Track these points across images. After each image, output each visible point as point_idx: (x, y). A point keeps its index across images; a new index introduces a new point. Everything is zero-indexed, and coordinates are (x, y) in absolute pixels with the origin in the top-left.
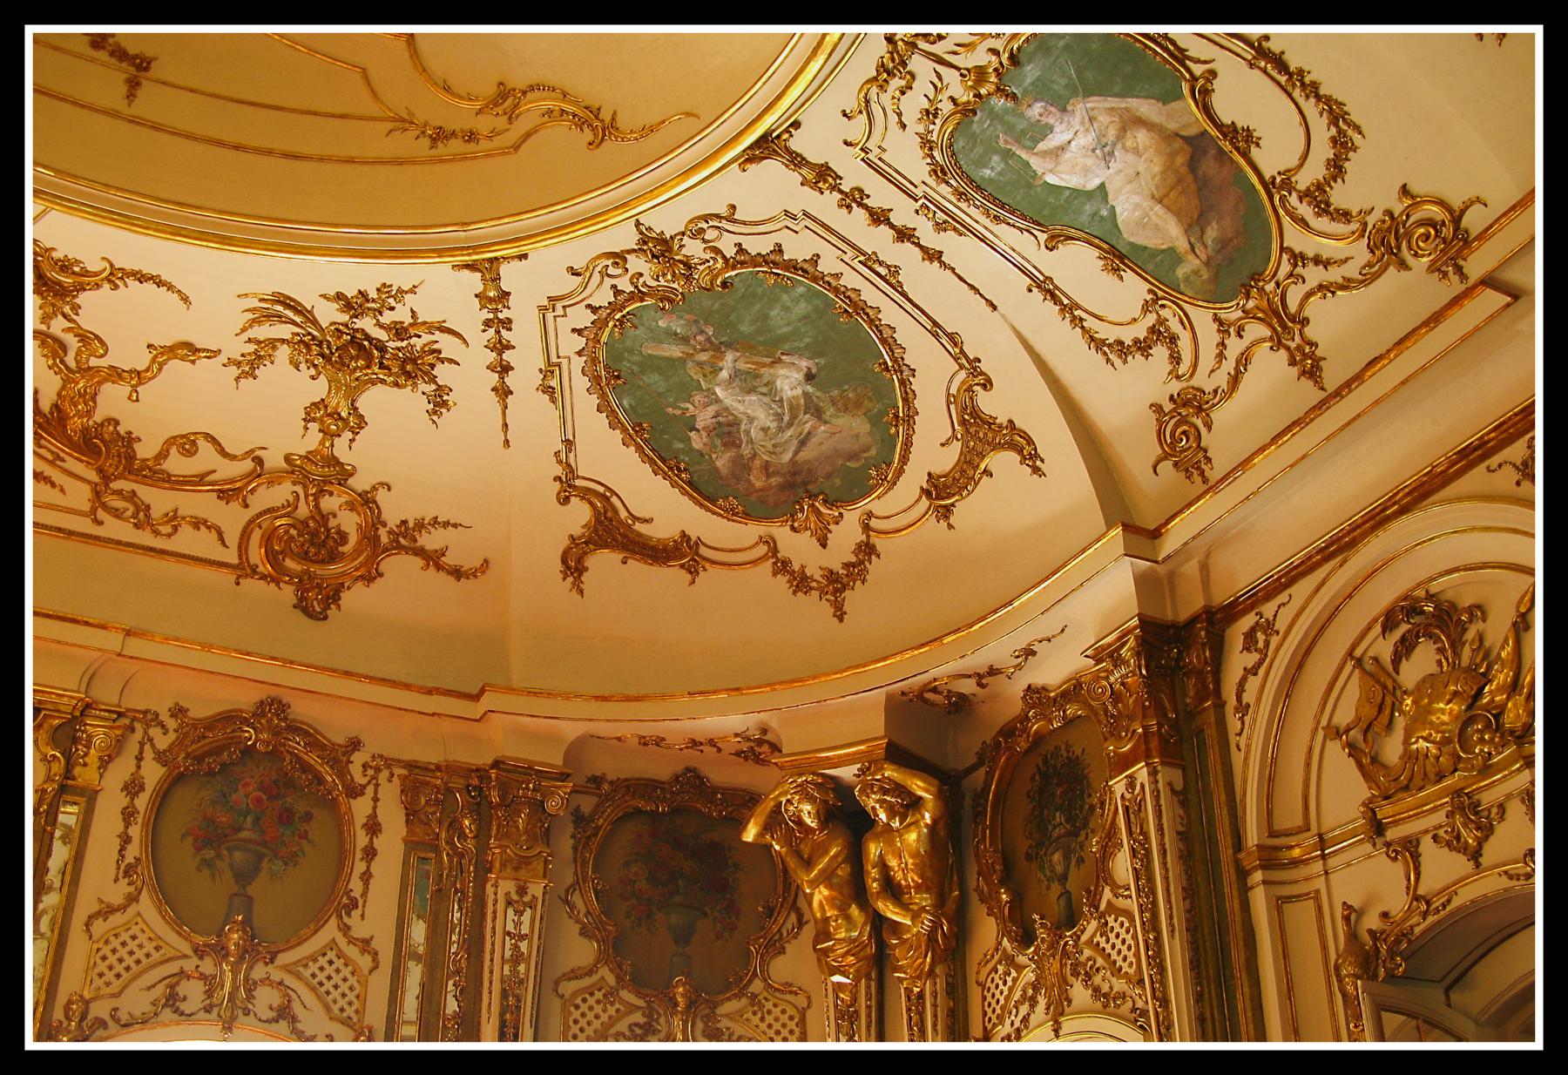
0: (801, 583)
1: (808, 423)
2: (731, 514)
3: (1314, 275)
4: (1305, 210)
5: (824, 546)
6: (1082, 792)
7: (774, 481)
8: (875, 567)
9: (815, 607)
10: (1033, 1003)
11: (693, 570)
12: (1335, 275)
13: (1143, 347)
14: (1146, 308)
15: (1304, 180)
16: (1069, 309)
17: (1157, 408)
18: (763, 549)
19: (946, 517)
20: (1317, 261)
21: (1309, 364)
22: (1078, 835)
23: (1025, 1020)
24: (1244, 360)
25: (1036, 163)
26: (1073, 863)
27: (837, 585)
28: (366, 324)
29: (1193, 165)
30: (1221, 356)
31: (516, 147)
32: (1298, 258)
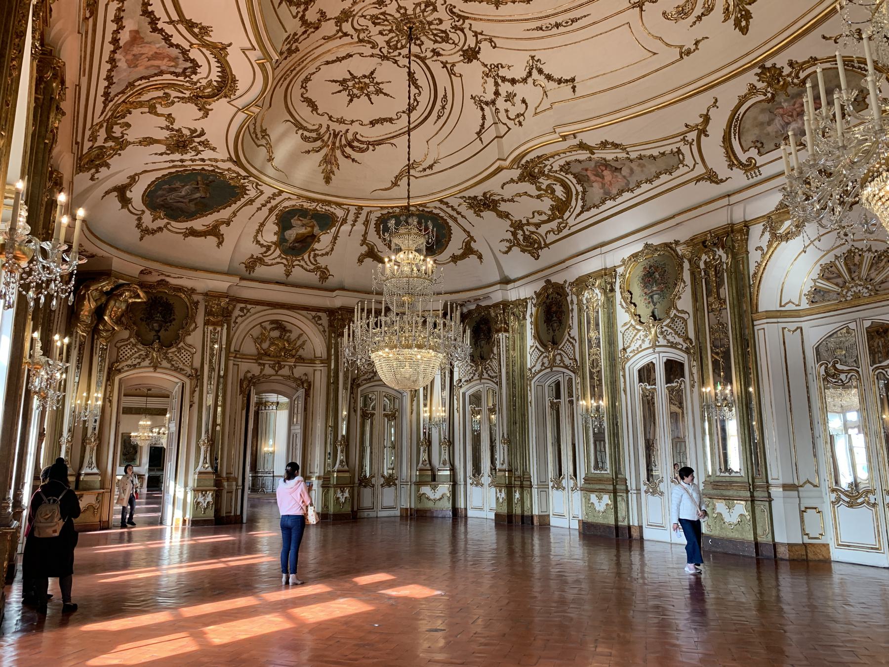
0: (139, 226)
1: (187, 201)
3: (302, 263)
4: (312, 255)
6: (171, 313)
7: (162, 203)
8: (158, 235)
9: (138, 233)
10: (144, 359)
11: (122, 208)
12: (305, 266)
13: (262, 246)
14: (272, 242)
15: (317, 252)
16: (259, 231)
17: (252, 255)
18: (140, 212)
19: (185, 237)
21: (288, 273)
22: (167, 323)
23: (139, 363)
24: (278, 263)
25: (296, 218)
26: (163, 329)
27: (146, 231)
29: (308, 236)
30: (274, 259)
32: (303, 259)
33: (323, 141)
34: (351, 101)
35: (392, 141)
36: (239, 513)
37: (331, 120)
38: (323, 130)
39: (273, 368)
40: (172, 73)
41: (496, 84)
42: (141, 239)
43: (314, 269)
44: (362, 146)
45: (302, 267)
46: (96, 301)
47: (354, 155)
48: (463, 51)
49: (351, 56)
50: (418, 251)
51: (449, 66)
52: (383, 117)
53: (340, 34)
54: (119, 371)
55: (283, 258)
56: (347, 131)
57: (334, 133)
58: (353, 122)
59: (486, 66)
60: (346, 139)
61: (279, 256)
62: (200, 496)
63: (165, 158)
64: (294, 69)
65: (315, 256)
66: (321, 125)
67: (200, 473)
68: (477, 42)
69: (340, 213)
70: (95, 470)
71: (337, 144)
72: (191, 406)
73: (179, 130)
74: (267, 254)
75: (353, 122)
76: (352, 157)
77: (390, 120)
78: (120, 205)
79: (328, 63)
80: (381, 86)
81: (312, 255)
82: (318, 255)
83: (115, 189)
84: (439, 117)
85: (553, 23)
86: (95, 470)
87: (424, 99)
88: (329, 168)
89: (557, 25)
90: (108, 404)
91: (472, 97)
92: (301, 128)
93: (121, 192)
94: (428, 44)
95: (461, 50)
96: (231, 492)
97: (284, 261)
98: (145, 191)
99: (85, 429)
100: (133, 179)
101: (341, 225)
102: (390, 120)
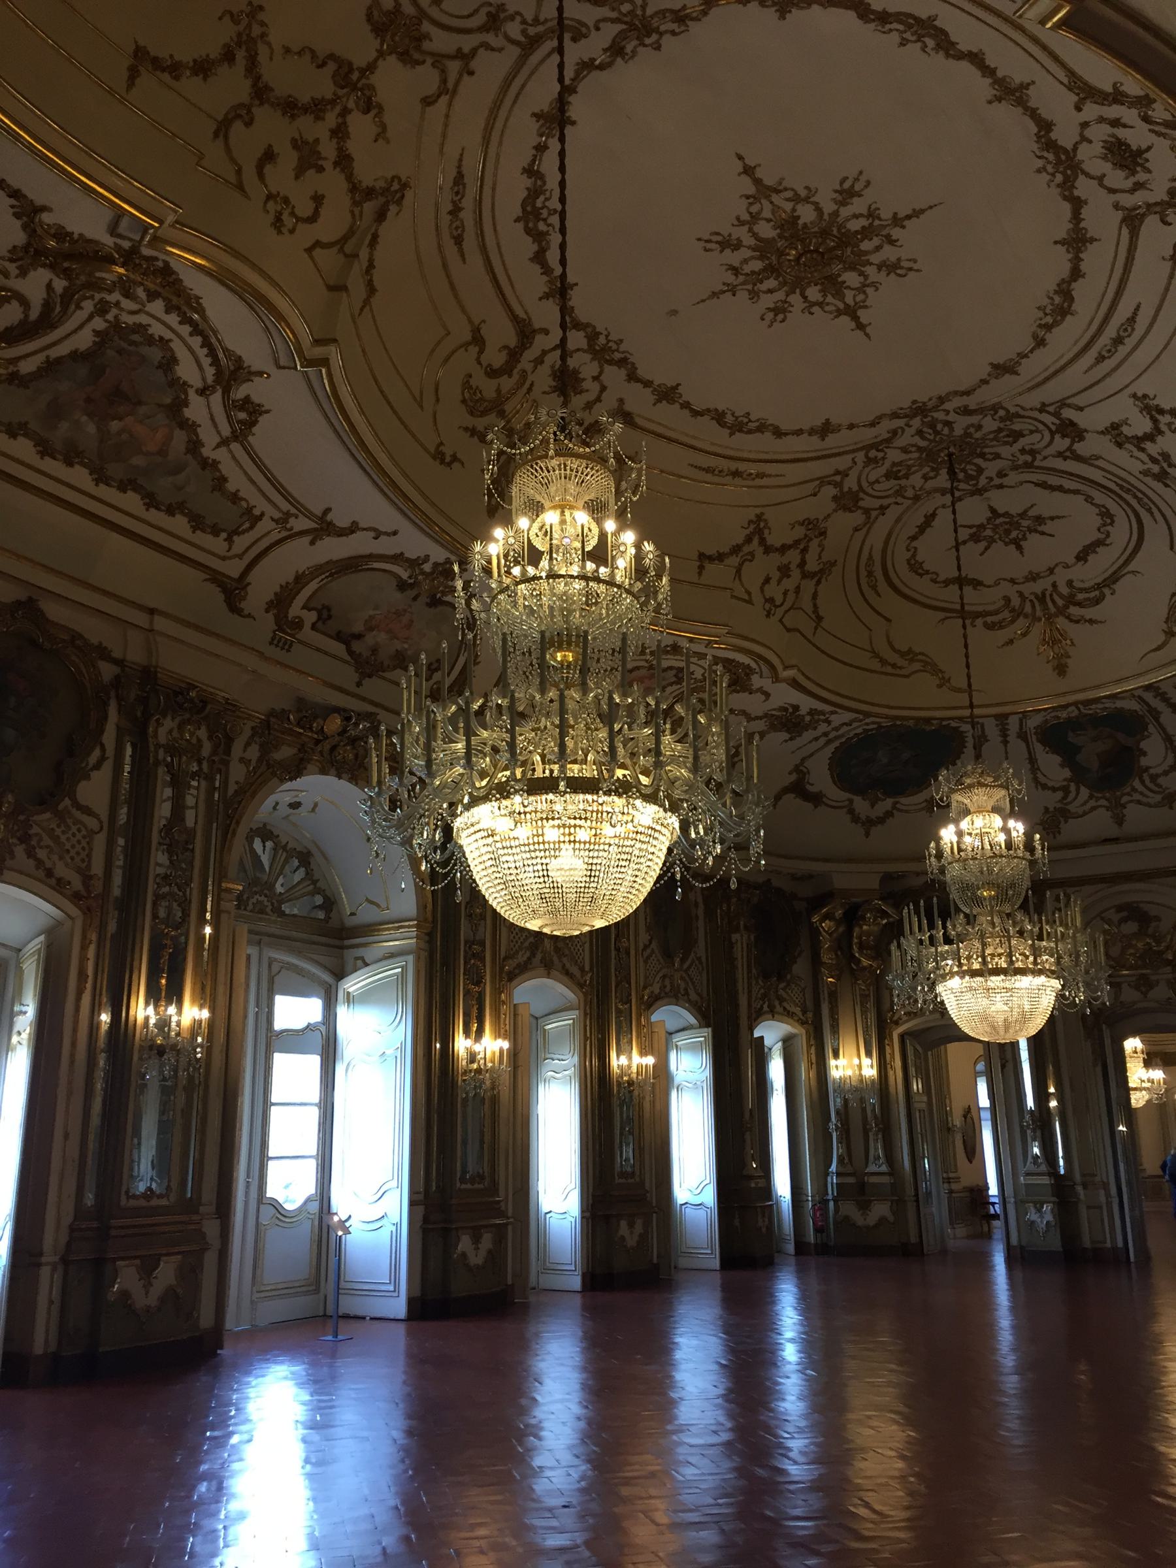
0: (856, 819)
2: (843, 789)
5: (873, 806)
12: (1144, 800)
13: (1054, 789)
14: (1065, 780)
15: (1152, 771)
17: (1047, 809)
20: (1141, 793)
21: (1120, 821)
24: (1094, 809)
25: (1070, 734)
27: (869, 824)
28: (808, 718)
31: (371, 289)
32: (1134, 790)
33: (1026, 616)
34: (1019, 548)
35: (1131, 567)
36: (1120, 1244)
37: (1015, 583)
38: (1016, 602)
39: (1137, 988)
40: (671, 684)
41: (1143, 450)
42: (867, 834)
43: (1163, 799)
44: (1092, 595)
45: (1139, 802)
46: (830, 935)
47: (1089, 613)
48: (1057, 431)
49: (934, 515)
50: (996, 810)
51: (1068, 454)
52: (1087, 542)
53: (874, 514)
54: (897, 1023)
55: (1098, 799)
56: (1054, 585)
57: (1037, 597)
58: (1051, 571)
59: (1102, 433)
60: (1061, 596)
61: (1091, 797)
62: (1033, 1210)
63: (799, 742)
64: (870, 574)
65: (1154, 778)
66: (1007, 600)
67: (1028, 1174)
68: (1057, 414)
69: (1133, 705)
70: (884, 1168)
71: (1053, 610)
72: (1003, 1066)
73: (766, 715)
74: (1069, 799)
75: (1051, 571)
76: (1088, 617)
77: (1099, 543)
78: (810, 806)
79: (914, 538)
80: (1031, 513)
81: (1145, 775)
82: (1158, 776)
83: (787, 790)
84: (1149, 511)
85: (1109, 342)
86: (884, 1168)
87: (1099, 497)
88: (1057, 651)
89: (1118, 341)
90: (891, 1073)
91: (1146, 473)
92: (978, 617)
93: (799, 788)
94: (1005, 451)
95: (1052, 433)
96: (1100, 1208)
97: (1103, 802)
98: (832, 777)
99: (864, 1110)
100: (800, 771)
101: (1157, 719)
102: (1099, 543)
